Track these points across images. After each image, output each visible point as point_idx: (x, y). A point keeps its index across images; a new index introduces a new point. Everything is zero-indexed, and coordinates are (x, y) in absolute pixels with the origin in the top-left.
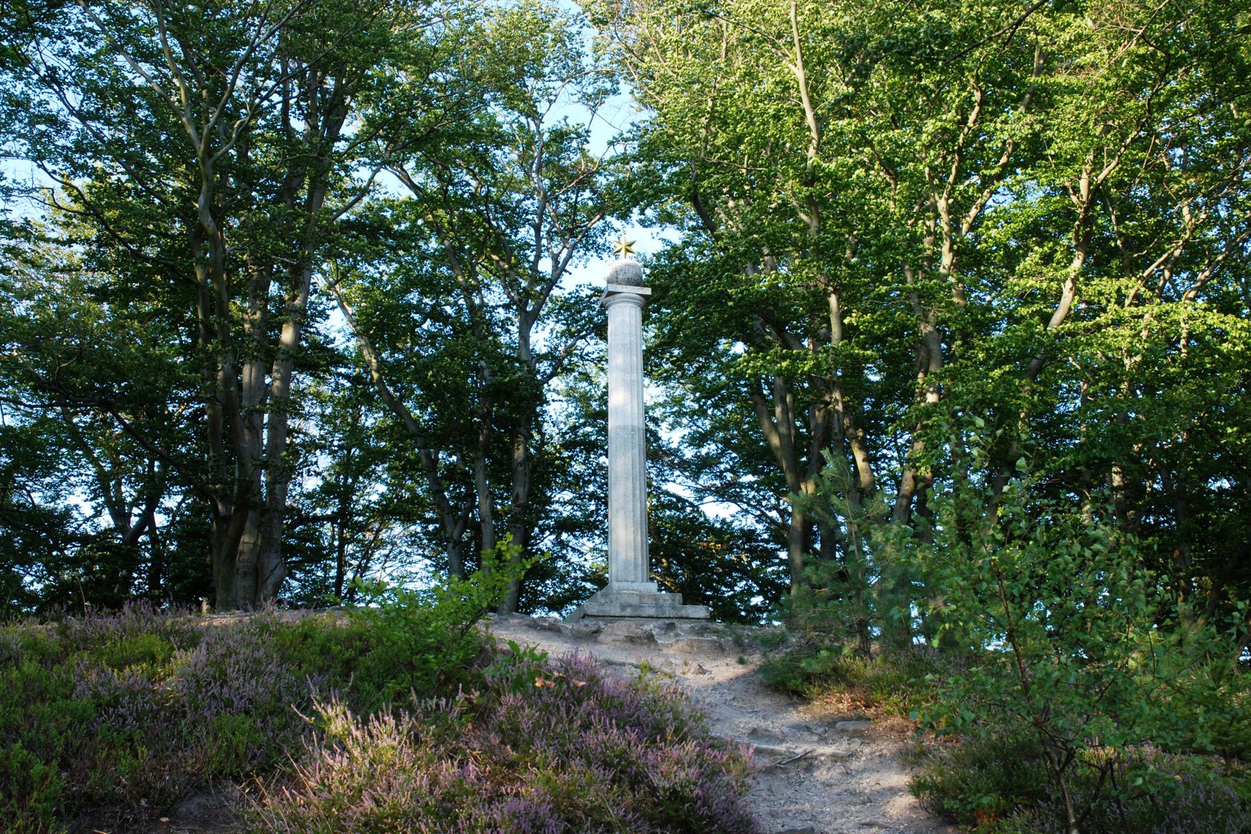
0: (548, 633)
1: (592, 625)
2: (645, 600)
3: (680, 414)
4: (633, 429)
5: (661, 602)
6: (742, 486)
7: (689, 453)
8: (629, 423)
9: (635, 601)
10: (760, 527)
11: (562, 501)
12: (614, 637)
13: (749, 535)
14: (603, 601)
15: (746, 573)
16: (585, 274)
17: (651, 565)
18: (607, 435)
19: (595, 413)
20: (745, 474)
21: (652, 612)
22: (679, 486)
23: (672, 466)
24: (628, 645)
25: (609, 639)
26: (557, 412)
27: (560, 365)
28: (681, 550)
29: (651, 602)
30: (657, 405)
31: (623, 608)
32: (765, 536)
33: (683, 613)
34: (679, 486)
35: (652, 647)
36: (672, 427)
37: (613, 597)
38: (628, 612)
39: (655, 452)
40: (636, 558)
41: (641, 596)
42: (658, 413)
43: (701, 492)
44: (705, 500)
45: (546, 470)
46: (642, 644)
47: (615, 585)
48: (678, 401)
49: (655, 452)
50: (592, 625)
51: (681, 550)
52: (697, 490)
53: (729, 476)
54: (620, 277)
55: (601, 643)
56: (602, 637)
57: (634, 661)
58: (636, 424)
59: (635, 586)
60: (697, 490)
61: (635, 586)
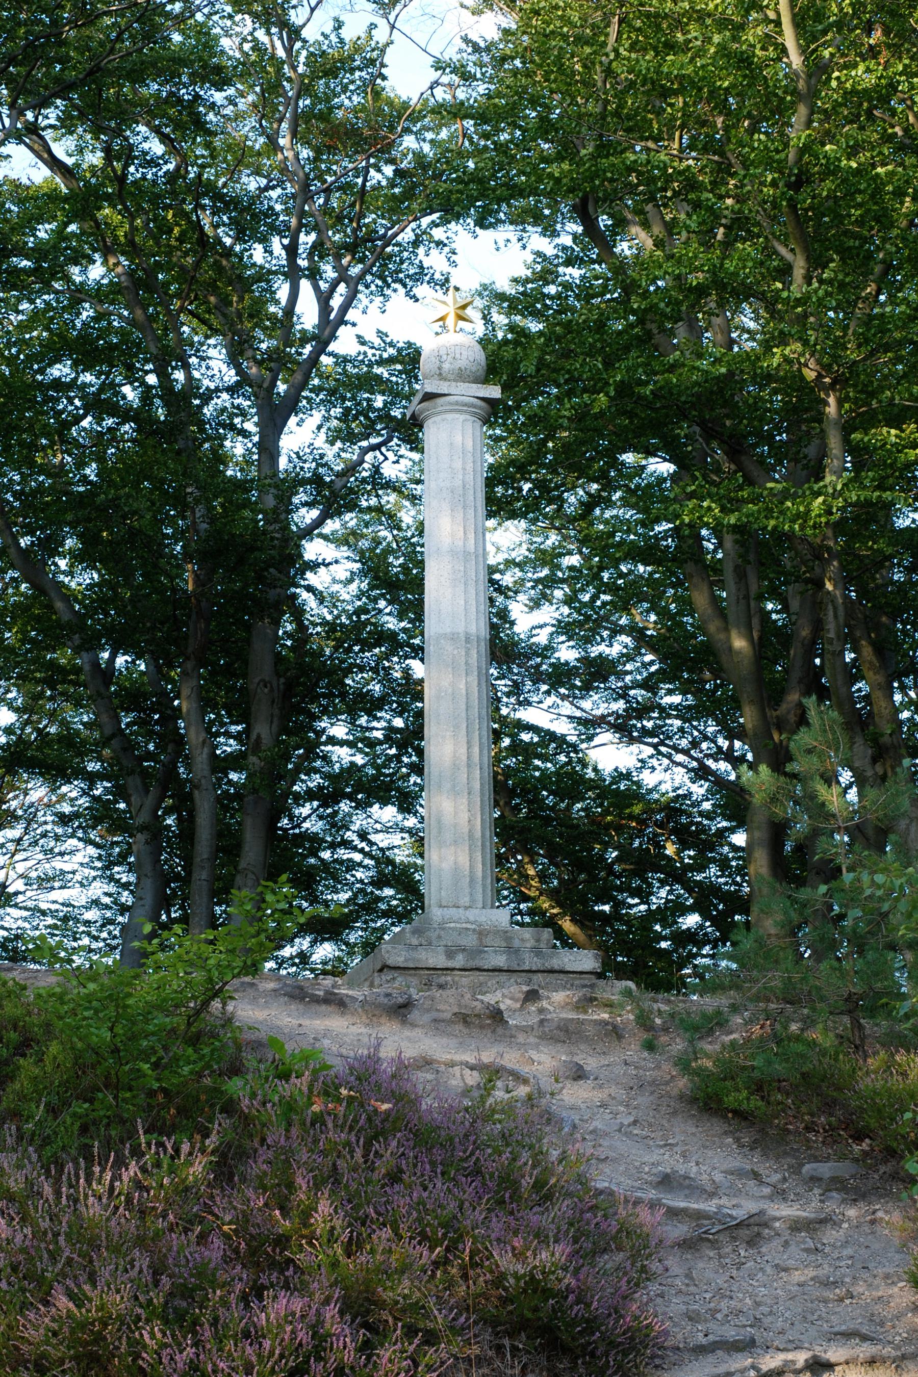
0: (324, 1007)
1: (397, 987)
2: (488, 941)
3: (550, 582)
4: (468, 640)
5: (516, 943)
6: (664, 712)
7: (567, 654)
8: (461, 629)
9: (470, 941)
10: (699, 790)
11: (340, 743)
12: (435, 1015)
13: (673, 810)
14: (415, 941)
15: (676, 875)
16: (382, 321)
17: (499, 856)
18: (420, 617)
19: (398, 580)
20: (670, 692)
21: (500, 961)
22: (547, 713)
23: (537, 677)
24: (459, 1027)
25: (427, 1018)
26: (330, 574)
27: (335, 495)
28: (551, 825)
29: (499, 942)
30: (510, 563)
31: (450, 954)
32: (707, 806)
33: (555, 963)
34: (547, 713)
35: (500, 1030)
36: (536, 604)
37: (433, 935)
38: (460, 961)
39: (503, 649)
40: (471, 867)
41: (481, 933)
42: (508, 579)
43: (589, 725)
44: (597, 740)
45: (309, 682)
46: (482, 1027)
47: (436, 913)
48: (547, 558)
49: (503, 649)
50: (397, 987)
51: (551, 825)
52: (580, 721)
53: (638, 694)
54: (446, 366)
55: (414, 1025)
56: (414, 1015)
57: (470, 1058)
58: (473, 629)
59: (472, 914)
60: (580, 721)
61: (472, 914)
